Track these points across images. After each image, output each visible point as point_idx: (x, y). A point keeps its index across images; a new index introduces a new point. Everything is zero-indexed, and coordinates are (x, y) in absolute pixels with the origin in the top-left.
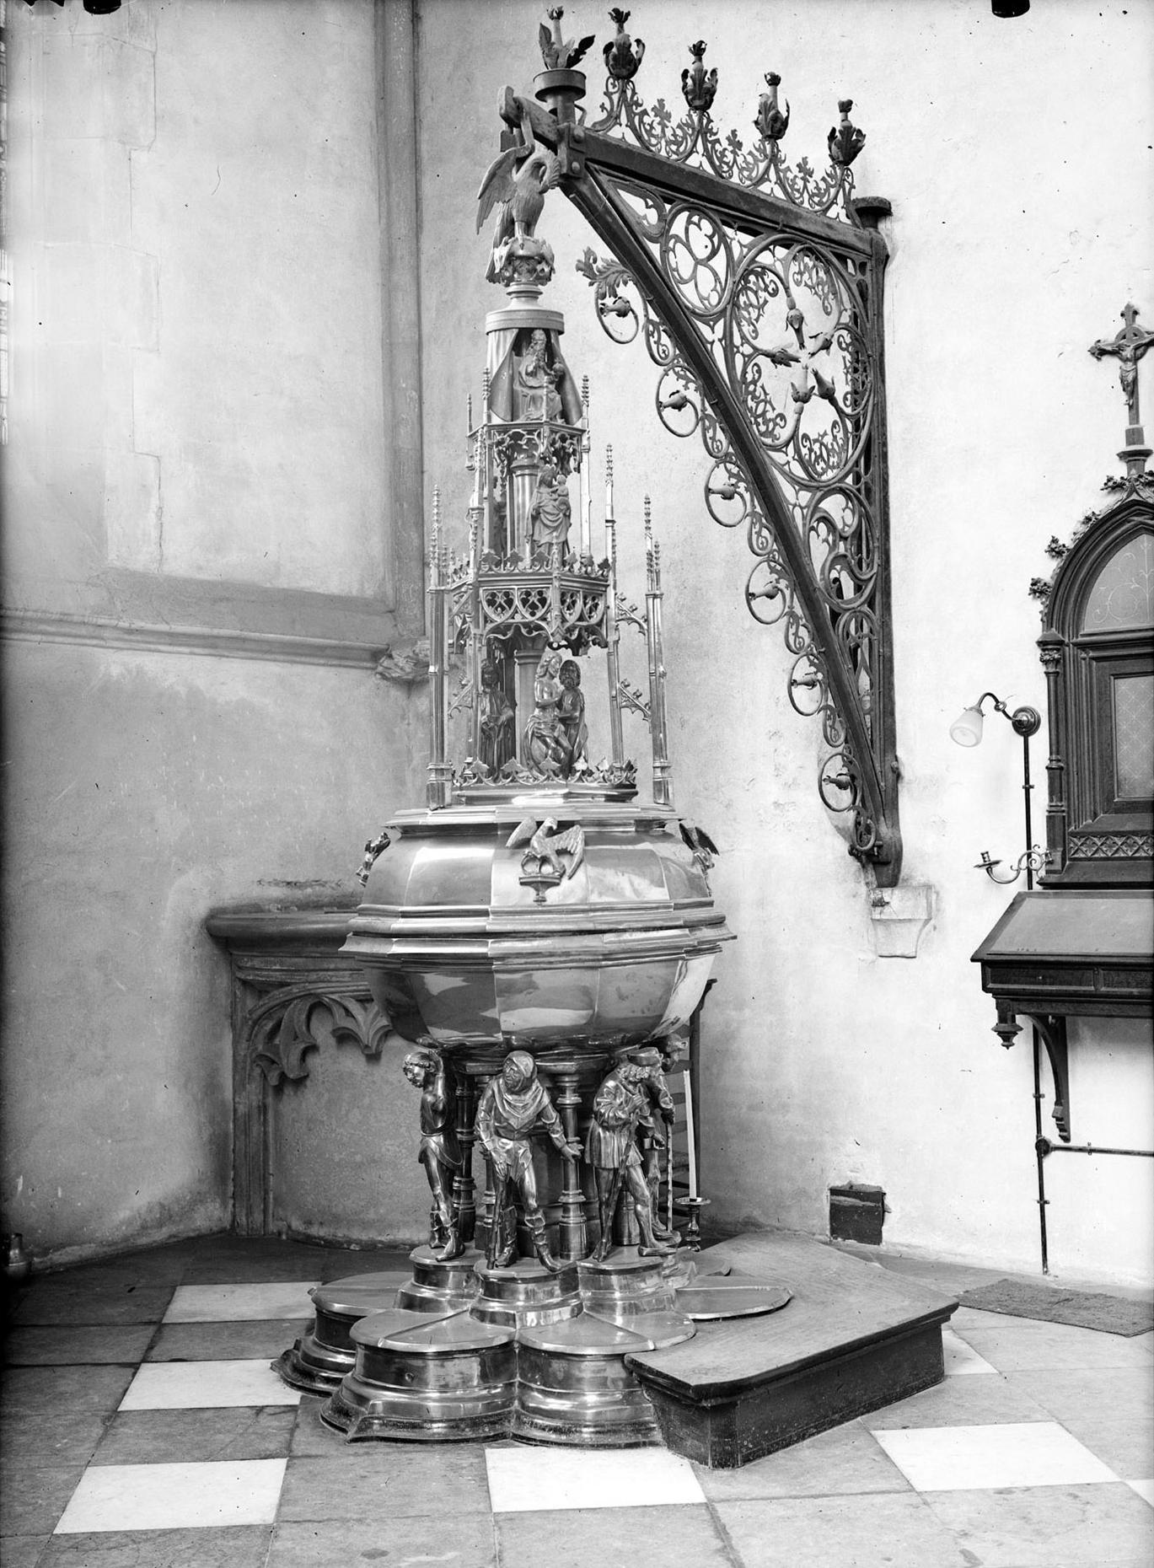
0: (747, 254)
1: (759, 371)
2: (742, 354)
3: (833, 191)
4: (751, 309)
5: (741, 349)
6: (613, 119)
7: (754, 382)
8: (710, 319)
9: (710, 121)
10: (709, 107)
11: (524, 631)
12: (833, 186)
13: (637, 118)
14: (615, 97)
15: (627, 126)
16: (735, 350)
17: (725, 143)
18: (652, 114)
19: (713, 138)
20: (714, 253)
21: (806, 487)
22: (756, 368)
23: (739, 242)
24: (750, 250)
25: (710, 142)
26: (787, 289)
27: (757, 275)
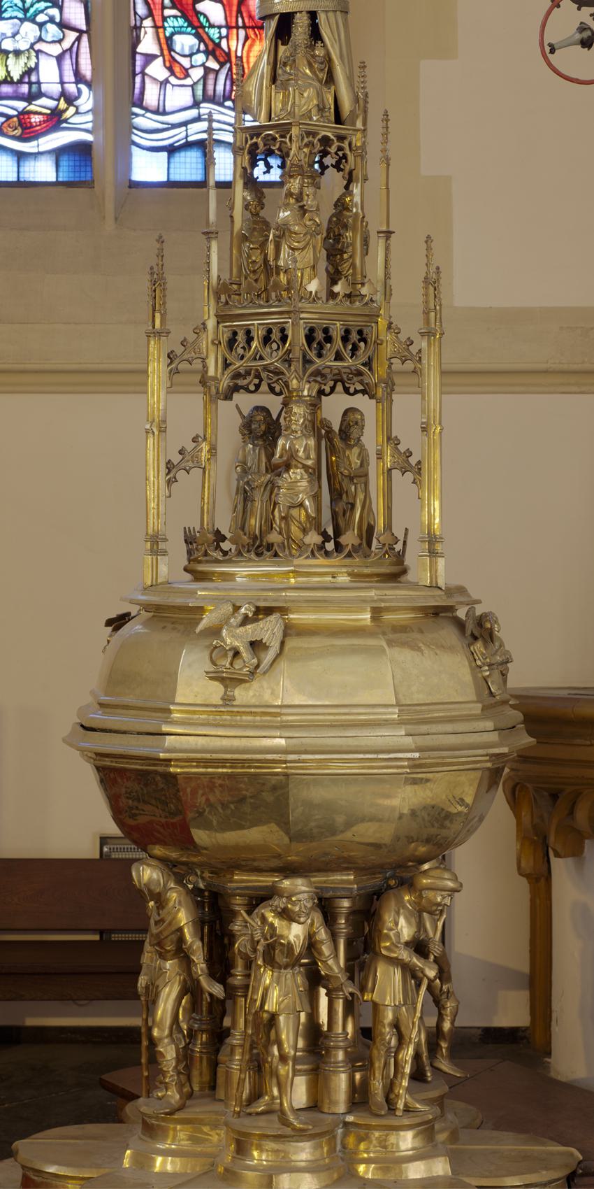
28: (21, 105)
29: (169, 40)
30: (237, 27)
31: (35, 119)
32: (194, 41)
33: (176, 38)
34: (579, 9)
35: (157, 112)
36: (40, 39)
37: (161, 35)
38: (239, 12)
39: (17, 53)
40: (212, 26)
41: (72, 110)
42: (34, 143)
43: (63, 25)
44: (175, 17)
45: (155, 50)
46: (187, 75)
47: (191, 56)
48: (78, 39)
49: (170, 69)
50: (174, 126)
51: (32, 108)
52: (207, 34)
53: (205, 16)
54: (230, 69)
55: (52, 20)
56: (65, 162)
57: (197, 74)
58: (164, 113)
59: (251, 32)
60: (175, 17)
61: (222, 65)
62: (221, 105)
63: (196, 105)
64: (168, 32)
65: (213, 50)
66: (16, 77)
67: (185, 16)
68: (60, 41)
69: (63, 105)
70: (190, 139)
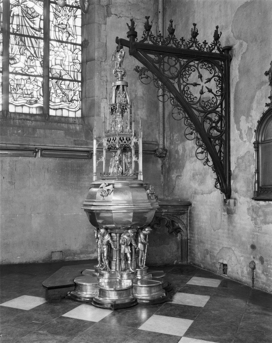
1: (189, 88)
2: (183, 85)
3: (213, 47)
4: (186, 75)
6: (145, 39)
7: (187, 90)
8: (173, 78)
9: (174, 36)
12: (213, 46)
13: (152, 39)
14: (146, 35)
15: (149, 40)
17: (179, 40)
19: (175, 40)
20: (176, 64)
21: (202, 112)
22: (188, 87)
27: (188, 67)
28: (30, 99)
29: (56, 90)
30: (68, 90)
31: (32, 101)
32: (60, 91)
33: (57, 90)
35: (54, 103)
36: (34, 88)
38: (68, 87)
39: (29, 90)
41: (39, 100)
42: (32, 105)
43: (37, 86)
45: (54, 92)
46: (59, 97)
48: (40, 88)
49: (56, 95)
50: (57, 105)
51: (32, 99)
55: (36, 85)
56: (38, 109)
57: (61, 97)
58: (55, 103)
59: (70, 91)
61: (65, 96)
63: (61, 102)
64: (56, 89)
66: (29, 94)
67: (59, 87)
68: (37, 88)
69: (37, 99)
70: (60, 108)
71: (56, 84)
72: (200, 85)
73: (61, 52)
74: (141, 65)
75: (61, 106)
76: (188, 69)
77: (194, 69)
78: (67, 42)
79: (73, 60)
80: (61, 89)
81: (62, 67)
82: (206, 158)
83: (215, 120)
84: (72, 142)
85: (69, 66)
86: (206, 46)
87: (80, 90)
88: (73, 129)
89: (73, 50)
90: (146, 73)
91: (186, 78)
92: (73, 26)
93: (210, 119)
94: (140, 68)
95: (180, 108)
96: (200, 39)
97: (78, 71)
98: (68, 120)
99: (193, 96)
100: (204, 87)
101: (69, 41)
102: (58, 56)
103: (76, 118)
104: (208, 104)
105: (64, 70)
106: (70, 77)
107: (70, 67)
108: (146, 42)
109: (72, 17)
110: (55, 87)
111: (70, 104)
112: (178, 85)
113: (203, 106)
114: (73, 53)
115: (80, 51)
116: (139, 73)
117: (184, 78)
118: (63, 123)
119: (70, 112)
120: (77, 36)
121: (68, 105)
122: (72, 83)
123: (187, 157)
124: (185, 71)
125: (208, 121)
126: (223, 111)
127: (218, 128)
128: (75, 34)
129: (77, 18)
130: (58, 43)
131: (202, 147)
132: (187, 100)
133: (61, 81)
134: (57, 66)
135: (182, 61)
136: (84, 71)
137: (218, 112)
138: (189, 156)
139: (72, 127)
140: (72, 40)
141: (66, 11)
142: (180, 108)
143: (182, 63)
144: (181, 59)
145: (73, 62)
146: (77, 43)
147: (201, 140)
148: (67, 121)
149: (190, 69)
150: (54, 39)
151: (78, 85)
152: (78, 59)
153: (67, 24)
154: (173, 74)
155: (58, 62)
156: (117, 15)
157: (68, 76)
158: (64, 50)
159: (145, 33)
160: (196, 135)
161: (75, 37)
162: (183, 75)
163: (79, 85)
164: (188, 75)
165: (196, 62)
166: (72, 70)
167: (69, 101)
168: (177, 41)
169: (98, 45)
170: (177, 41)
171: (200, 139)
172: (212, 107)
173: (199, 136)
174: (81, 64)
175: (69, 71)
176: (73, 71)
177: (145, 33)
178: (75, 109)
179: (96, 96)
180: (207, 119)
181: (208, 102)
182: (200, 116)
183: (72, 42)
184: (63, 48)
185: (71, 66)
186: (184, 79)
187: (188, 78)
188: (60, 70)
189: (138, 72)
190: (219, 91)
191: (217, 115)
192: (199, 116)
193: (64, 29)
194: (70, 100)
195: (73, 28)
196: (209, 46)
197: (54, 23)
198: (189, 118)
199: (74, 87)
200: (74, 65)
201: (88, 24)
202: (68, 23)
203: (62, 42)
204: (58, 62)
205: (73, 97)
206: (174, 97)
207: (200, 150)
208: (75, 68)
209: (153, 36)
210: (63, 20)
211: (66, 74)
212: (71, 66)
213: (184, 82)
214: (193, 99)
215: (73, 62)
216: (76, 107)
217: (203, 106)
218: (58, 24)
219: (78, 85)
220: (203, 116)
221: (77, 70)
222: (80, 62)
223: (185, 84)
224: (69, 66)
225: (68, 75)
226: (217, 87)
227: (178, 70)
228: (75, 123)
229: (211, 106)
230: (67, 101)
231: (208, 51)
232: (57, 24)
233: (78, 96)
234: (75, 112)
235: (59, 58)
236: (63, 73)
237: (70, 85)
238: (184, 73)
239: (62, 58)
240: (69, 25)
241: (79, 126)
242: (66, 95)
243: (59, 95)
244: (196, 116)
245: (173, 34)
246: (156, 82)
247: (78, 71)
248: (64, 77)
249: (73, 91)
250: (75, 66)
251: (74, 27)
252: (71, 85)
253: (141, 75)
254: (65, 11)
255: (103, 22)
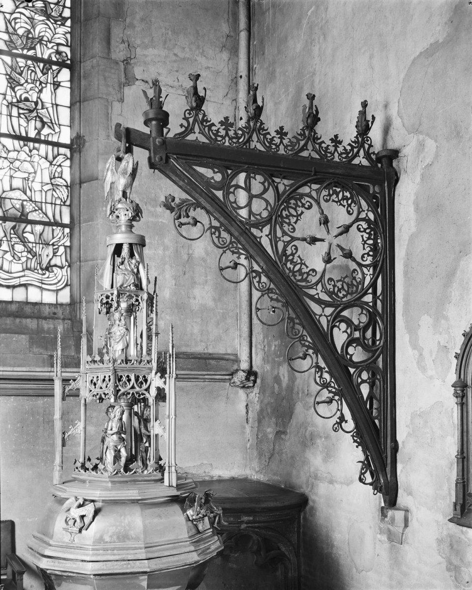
0: (289, 190)
1: (296, 249)
2: (283, 241)
3: (355, 150)
4: (291, 218)
5: (282, 239)
6: (189, 130)
7: (293, 254)
8: (259, 225)
9: (262, 123)
10: (260, 116)
11: (137, 396)
12: (356, 148)
13: (206, 129)
14: (191, 120)
15: (199, 133)
16: (278, 239)
18: (219, 126)
19: (264, 132)
20: (265, 190)
21: (327, 304)
22: (294, 247)
23: (283, 184)
24: (291, 188)
25: (262, 135)
26: (318, 204)
27: (296, 200)
29: (13, 246)
30: (39, 244)
33: (15, 245)
34: (233, 254)
35: (8, 272)
37: (10, 245)
38: (40, 237)
40: (29, 242)
44: (15, 238)
45: (7, 249)
46: (20, 260)
47: (21, 252)
49: (13, 257)
52: (28, 245)
53: (27, 238)
54: (37, 259)
57: (24, 259)
58: (11, 273)
59: (44, 246)
60: (15, 238)
61: (33, 257)
62: (33, 271)
63: (23, 270)
64: (13, 243)
65: (30, 251)
67: (19, 238)
70: (21, 283)
71: (12, 232)
72: (323, 240)
73: (25, 161)
74: (180, 195)
75: (23, 281)
76: (294, 204)
77: (310, 203)
78: (36, 140)
79: (51, 179)
80: (24, 241)
81: (26, 194)
82: (339, 413)
83: (360, 322)
84: (44, 358)
85: (41, 191)
86: (338, 149)
87: (68, 244)
88: (48, 332)
89: (50, 157)
90: (192, 213)
91: (289, 224)
92: (51, 105)
93: (349, 322)
94: (177, 201)
95: (275, 297)
96: (325, 131)
97: (62, 203)
98: (39, 311)
99: (307, 267)
100: (334, 247)
101: (43, 138)
102: (17, 170)
103: (58, 306)
104: (342, 285)
105: (31, 200)
106: (44, 216)
107: (44, 193)
108: (191, 137)
109: (49, 85)
110: (11, 238)
111: (44, 274)
112: (271, 240)
113: (332, 290)
114: (51, 163)
115: (68, 158)
116: (174, 213)
117: (285, 225)
118: (27, 317)
119: (45, 293)
120: (60, 128)
121: (40, 277)
122: (48, 229)
123: (298, 393)
124: (287, 208)
125: (343, 326)
126: (379, 303)
127: (366, 342)
128: (57, 123)
129: (60, 87)
130: (16, 142)
131: (330, 389)
132: (292, 278)
133: (23, 225)
134: (14, 191)
135: (280, 183)
136: (76, 202)
137: (366, 304)
138: (303, 392)
139: (46, 325)
140: (48, 135)
141: (36, 73)
142: (275, 297)
143: (281, 188)
144: (277, 180)
145: (52, 184)
146: (59, 141)
147: (326, 372)
148: (36, 311)
149: (300, 204)
150: (8, 133)
151: (63, 233)
152: (64, 177)
153: (39, 100)
154: (257, 215)
155: (17, 183)
156: (147, 82)
157: (40, 213)
158: (31, 157)
159: (187, 116)
160: (315, 361)
161: (57, 130)
162: (281, 216)
163: (65, 234)
164: (295, 216)
165: (315, 186)
166: (49, 200)
167: (42, 269)
168: (268, 136)
169: (106, 147)
170: (268, 136)
171: (324, 368)
172: (352, 294)
173: (322, 364)
174: (69, 188)
175: (43, 204)
176: (52, 203)
177: (187, 116)
178: (55, 286)
179: (99, 258)
180: (340, 321)
181: (344, 282)
182: (323, 314)
183: (50, 139)
184: (28, 152)
185: (46, 192)
186: (286, 227)
187: (294, 224)
188: (21, 201)
189: (172, 209)
190: (369, 255)
191: (364, 312)
192: (321, 315)
193: (31, 111)
194: (44, 266)
195: (50, 110)
196: (345, 149)
197: (9, 98)
198: (297, 321)
199: (53, 238)
200: (54, 190)
201: (84, 101)
202: (39, 98)
203: (26, 139)
204: (17, 183)
205: (51, 259)
206: (261, 271)
207: (325, 394)
208: (56, 196)
209: (208, 124)
210: (28, 92)
211: (36, 210)
212: (46, 192)
213: (284, 233)
214: (308, 274)
215: (52, 184)
216: (59, 281)
217: (332, 290)
218: (17, 100)
219: (63, 233)
220: (331, 315)
221: (62, 201)
222: (67, 182)
223: (287, 239)
224: (41, 191)
225: (40, 211)
226: (364, 245)
227: (270, 205)
228: (56, 316)
229: (350, 291)
230: (38, 268)
231: (344, 160)
232: (15, 100)
233: (63, 257)
234: (57, 291)
235: (19, 174)
236: (29, 207)
237: (45, 232)
238: (284, 213)
239: (26, 175)
240: (42, 102)
241: (64, 323)
242: (36, 255)
243: (20, 256)
244: (315, 314)
245: (259, 119)
246: (217, 234)
247: (62, 203)
248: (31, 217)
249: (51, 247)
250: (55, 191)
251: (55, 106)
252: (48, 234)
253: (179, 217)
254: (33, 71)
255: (115, 96)
